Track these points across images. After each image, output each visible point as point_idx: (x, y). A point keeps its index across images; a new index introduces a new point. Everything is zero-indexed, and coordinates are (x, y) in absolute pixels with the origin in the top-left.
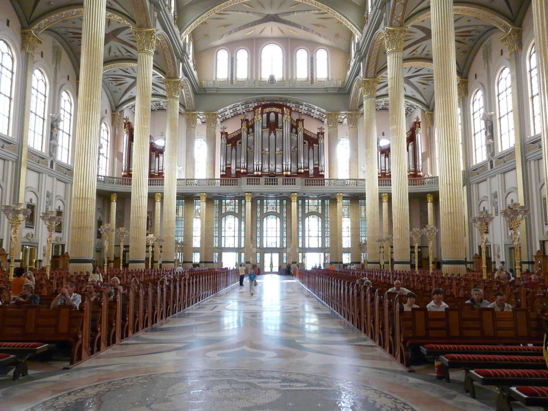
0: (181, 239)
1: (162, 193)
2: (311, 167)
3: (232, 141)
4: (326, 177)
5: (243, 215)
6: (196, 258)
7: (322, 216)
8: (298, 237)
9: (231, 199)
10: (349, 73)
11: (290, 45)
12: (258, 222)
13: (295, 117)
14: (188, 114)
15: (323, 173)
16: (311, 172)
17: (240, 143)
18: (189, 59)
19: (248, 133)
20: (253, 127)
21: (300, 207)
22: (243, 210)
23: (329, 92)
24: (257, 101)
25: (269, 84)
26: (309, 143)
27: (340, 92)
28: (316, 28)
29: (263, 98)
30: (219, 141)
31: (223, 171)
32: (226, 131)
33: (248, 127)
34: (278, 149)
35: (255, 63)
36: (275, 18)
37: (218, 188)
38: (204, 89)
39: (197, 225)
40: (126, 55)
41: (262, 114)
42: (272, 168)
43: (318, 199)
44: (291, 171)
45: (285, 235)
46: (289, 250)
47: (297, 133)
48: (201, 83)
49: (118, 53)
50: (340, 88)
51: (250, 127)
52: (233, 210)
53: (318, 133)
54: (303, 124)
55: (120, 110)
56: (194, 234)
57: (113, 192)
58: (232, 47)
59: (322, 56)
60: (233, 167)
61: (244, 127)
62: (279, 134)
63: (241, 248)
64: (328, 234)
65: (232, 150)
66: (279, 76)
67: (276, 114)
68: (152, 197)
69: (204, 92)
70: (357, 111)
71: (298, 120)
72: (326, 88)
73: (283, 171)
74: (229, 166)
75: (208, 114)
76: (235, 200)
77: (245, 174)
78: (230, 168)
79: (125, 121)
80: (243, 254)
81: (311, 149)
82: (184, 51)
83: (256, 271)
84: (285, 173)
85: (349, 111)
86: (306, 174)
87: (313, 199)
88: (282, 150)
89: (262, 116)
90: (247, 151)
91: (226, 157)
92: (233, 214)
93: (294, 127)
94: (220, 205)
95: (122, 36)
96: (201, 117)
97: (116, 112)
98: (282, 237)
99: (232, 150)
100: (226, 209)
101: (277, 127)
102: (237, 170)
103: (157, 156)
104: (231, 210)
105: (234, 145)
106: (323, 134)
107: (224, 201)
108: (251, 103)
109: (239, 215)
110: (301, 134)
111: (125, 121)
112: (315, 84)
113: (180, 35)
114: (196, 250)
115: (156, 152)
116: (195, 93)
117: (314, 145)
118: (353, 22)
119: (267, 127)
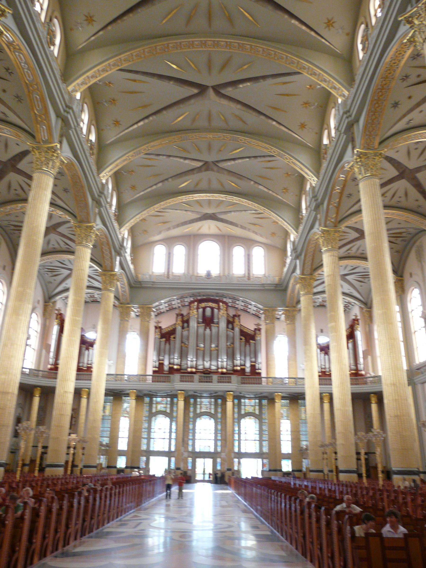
0: (105, 441)
1: (89, 389)
2: (248, 364)
3: (167, 336)
4: (264, 375)
5: (175, 414)
6: (121, 462)
7: (259, 417)
8: (234, 440)
9: (162, 397)
10: (285, 269)
11: (227, 241)
12: (191, 423)
13: (232, 312)
14: (122, 307)
15: (260, 371)
16: (248, 370)
17: (174, 338)
18: (126, 252)
19: (183, 328)
20: (187, 322)
21: (236, 407)
22: (175, 409)
23: (266, 288)
24: (193, 295)
25: (207, 280)
26: (246, 339)
27: (277, 288)
28: (252, 227)
29: (199, 293)
30: (153, 335)
31: (155, 367)
32: (160, 325)
33: (183, 322)
35: (191, 259)
36: (213, 217)
37: (149, 383)
38: (140, 282)
39: (124, 425)
40: (64, 247)
41: (198, 308)
42: (207, 365)
43: (255, 398)
44: (226, 369)
45: (219, 438)
46: (223, 455)
47: (233, 329)
48: (137, 276)
49: (56, 246)
50: (276, 284)
51: (185, 322)
53: (255, 329)
54: (239, 319)
55: (53, 300)
56: (121, 434)
57: (36, 386)
58: (169, 242)
59: (258, 253)
60: (166, 363)
61: (179, 322)
62: (214, 330)
63: (172, 452)
64: (266, 437)
66: (215, 271)
67: (212, 309)
68: (78, 393)
69: (139, 286)
70: (294, 307)
71: (235, 316)
72: (263, 284)
73: (218, 368)
75: (142, 308)
77: (178, 371)
79: (56, 312)
80: (173, 459)
82: (122, 246)
83: (185, 478)
85: (287, 307)
86: (242, 372)
87: (250, 398)
89: (197, 311)
90: (181, 347)
91: (159, 352)
92: (164, 413)
93: (230, 323)
94: (151, 404)
95: (61, 229)
96: (135, 310)
97: (48, 302)
98: (216, 440)
100: (156, 407)
101: (213, 323)
102: (171, 366)
103: (87, 349)
104: (163, 409)
105: (168, 340)
106: (259, 330)
107: (154, 399)
108: (187, 297)
109: (170, 415)
110: (237, 329)
111: (56, 312)
112: (252, 280)
113: (120, 229)
114: (122, 453)
115: (86, 344)
116: (131, 286)
117: (251, 341)
118: (289, 222)
119: (203, 322)
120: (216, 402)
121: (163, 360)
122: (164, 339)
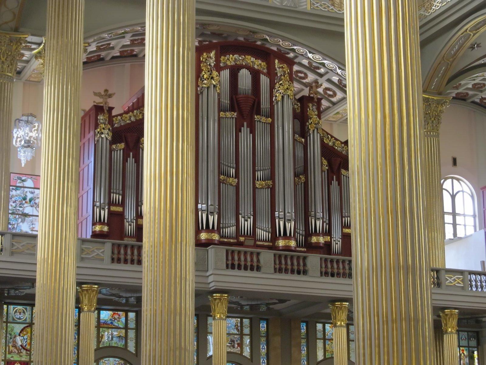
26: (330, 164)
31: (101, 222)
34: (259, 174)
42: (246, 224)
52: (121, 344)
65: (125, 160)
67: (255, 75)
73: (274, 237)
74: (120, 209)
76: (126, 312)
78: (121, 215)
81: (335, 183)
84: (281, 243)
88: (272, 177)
99: (125, 160)
101: (258, 113)
104: (116, 343)
119: (232, 109)
120: (253, 327)
121: (123, 204)
122: (122, 145)
